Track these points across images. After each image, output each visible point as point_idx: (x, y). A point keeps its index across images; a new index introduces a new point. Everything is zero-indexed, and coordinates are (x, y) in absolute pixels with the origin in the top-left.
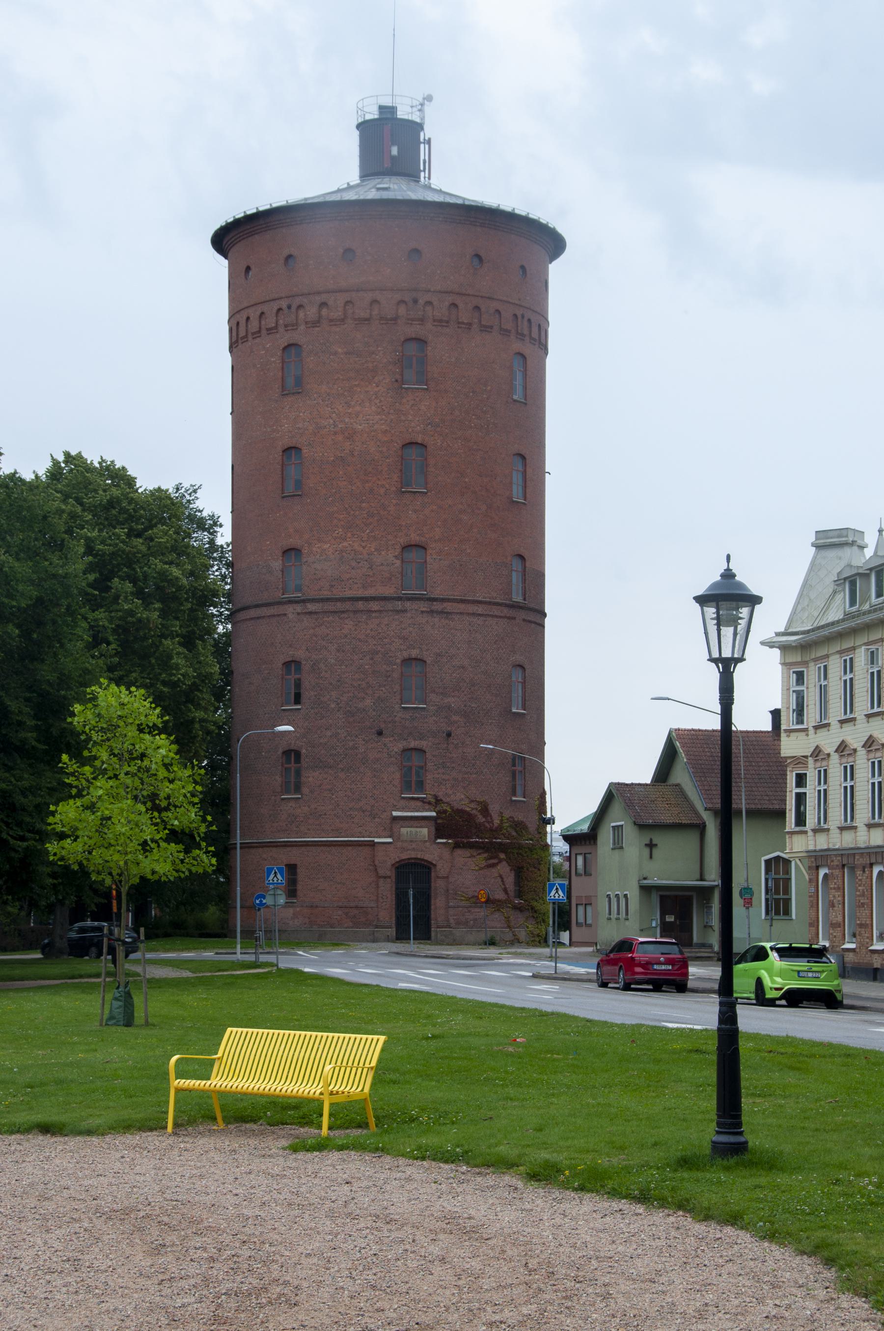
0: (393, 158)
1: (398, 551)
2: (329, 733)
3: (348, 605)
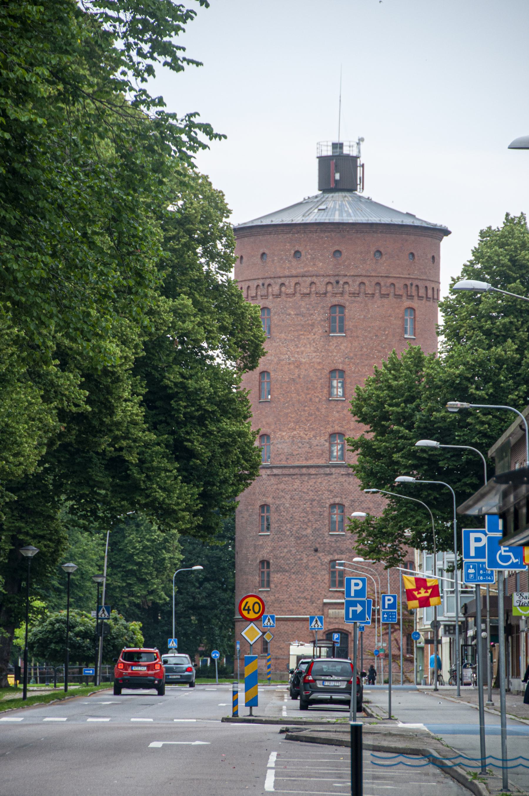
0: (336, 181)
1: (327, 437)
2: (286, 550)
3: (296, 471)
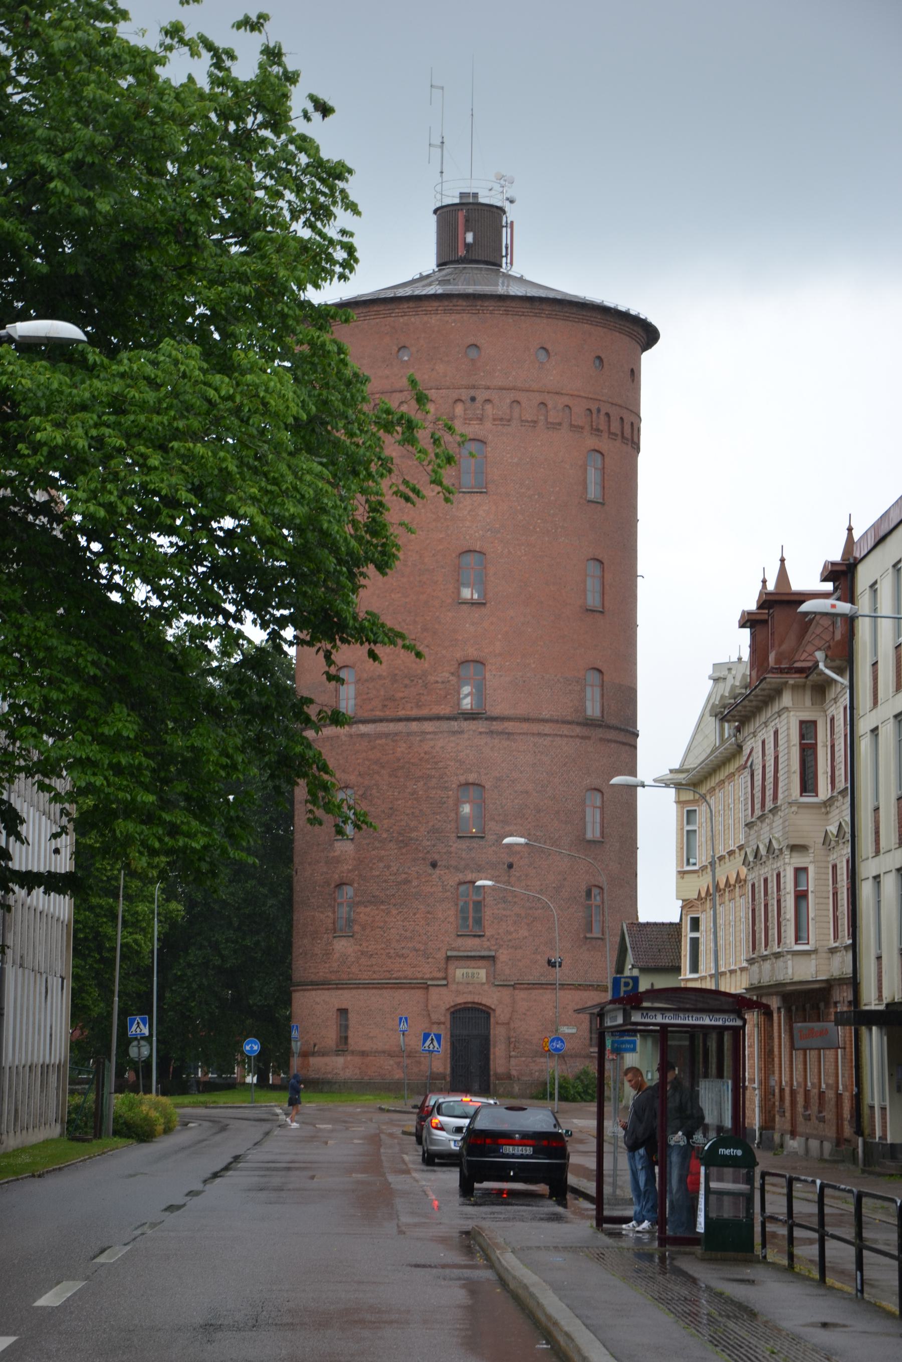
0: (467, 246)
2: (381, 865)
